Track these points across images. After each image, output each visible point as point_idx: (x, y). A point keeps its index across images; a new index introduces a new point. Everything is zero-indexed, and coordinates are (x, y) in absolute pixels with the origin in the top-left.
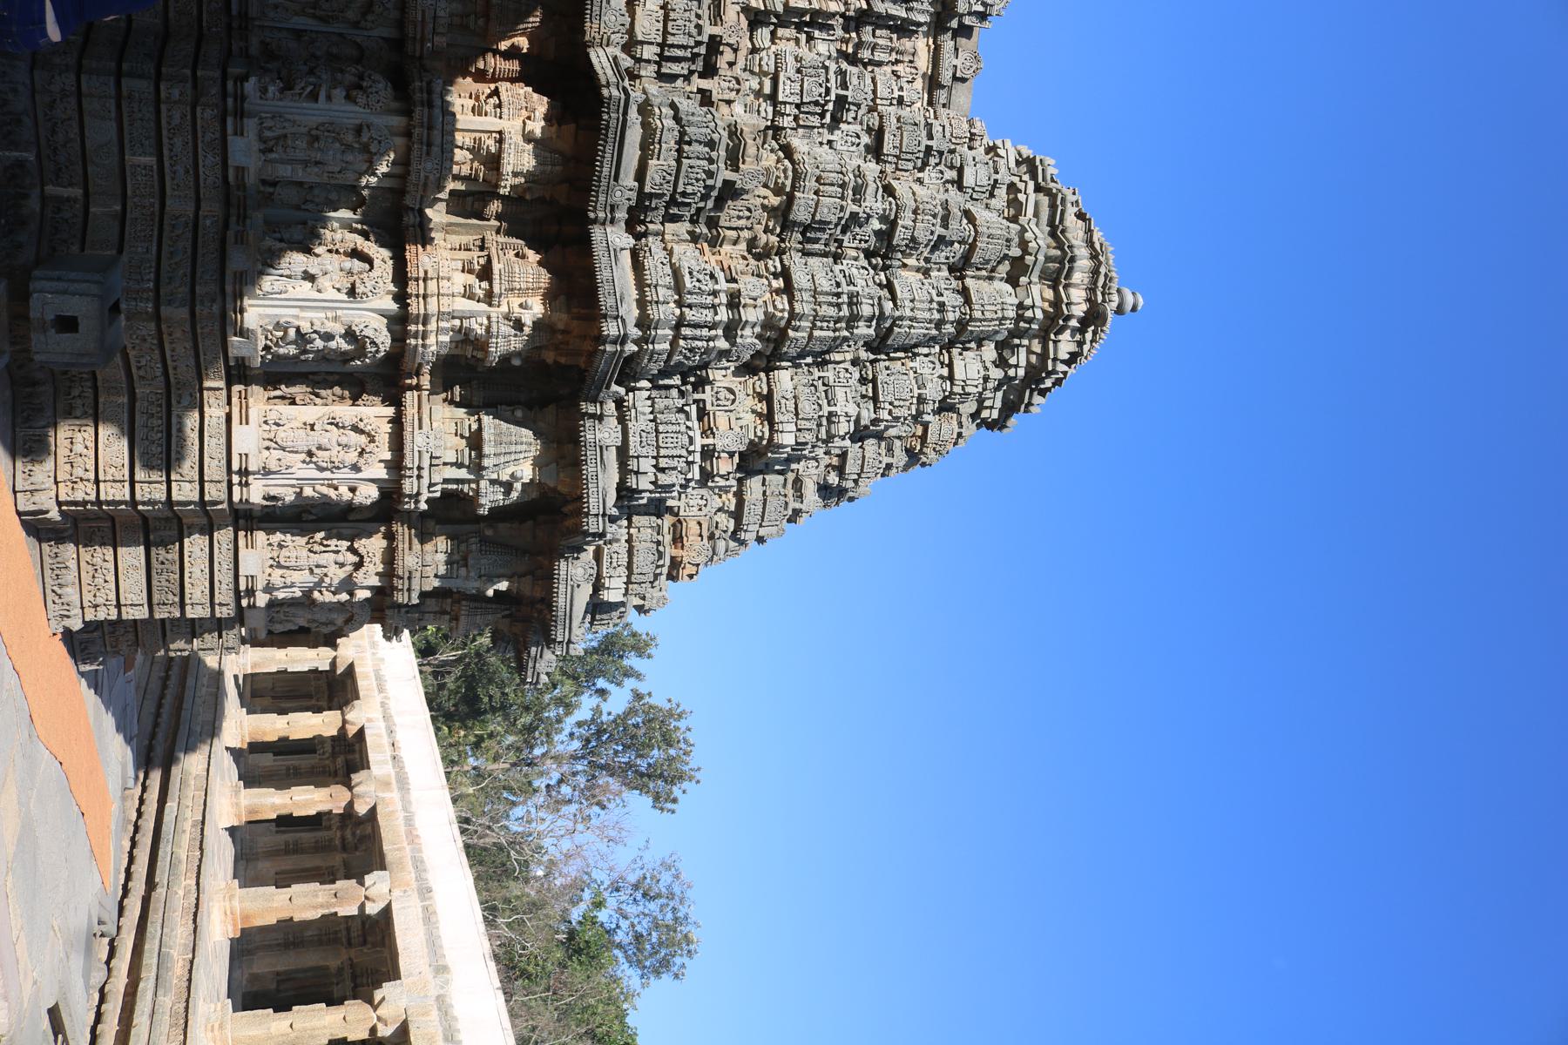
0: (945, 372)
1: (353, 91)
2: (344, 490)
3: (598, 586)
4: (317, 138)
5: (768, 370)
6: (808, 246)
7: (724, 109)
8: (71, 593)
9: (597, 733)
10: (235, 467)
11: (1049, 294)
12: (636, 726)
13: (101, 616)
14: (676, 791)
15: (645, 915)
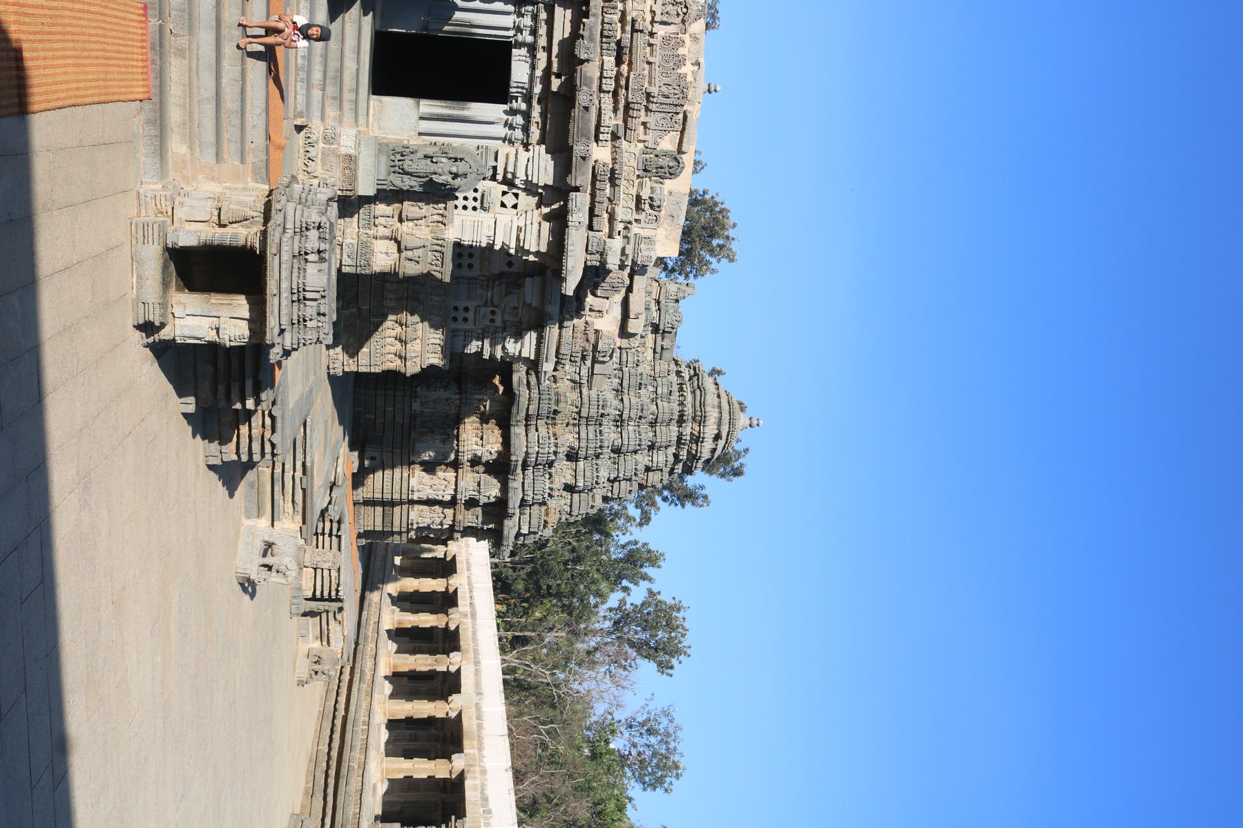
0: (650, 459)
1: (446, 388)
2: (440, 497)
3: (520, 528)
4: (435, 403)
5: (577, 461)
6: (589, 423)
7: (561, 381)
8: (361, 522)
9: (622, 619)
10: (410, 490)
11: (697, 429)
12: (648, 614)
13: (369, 529)
14: (674, 661)
15: (648, 746)
